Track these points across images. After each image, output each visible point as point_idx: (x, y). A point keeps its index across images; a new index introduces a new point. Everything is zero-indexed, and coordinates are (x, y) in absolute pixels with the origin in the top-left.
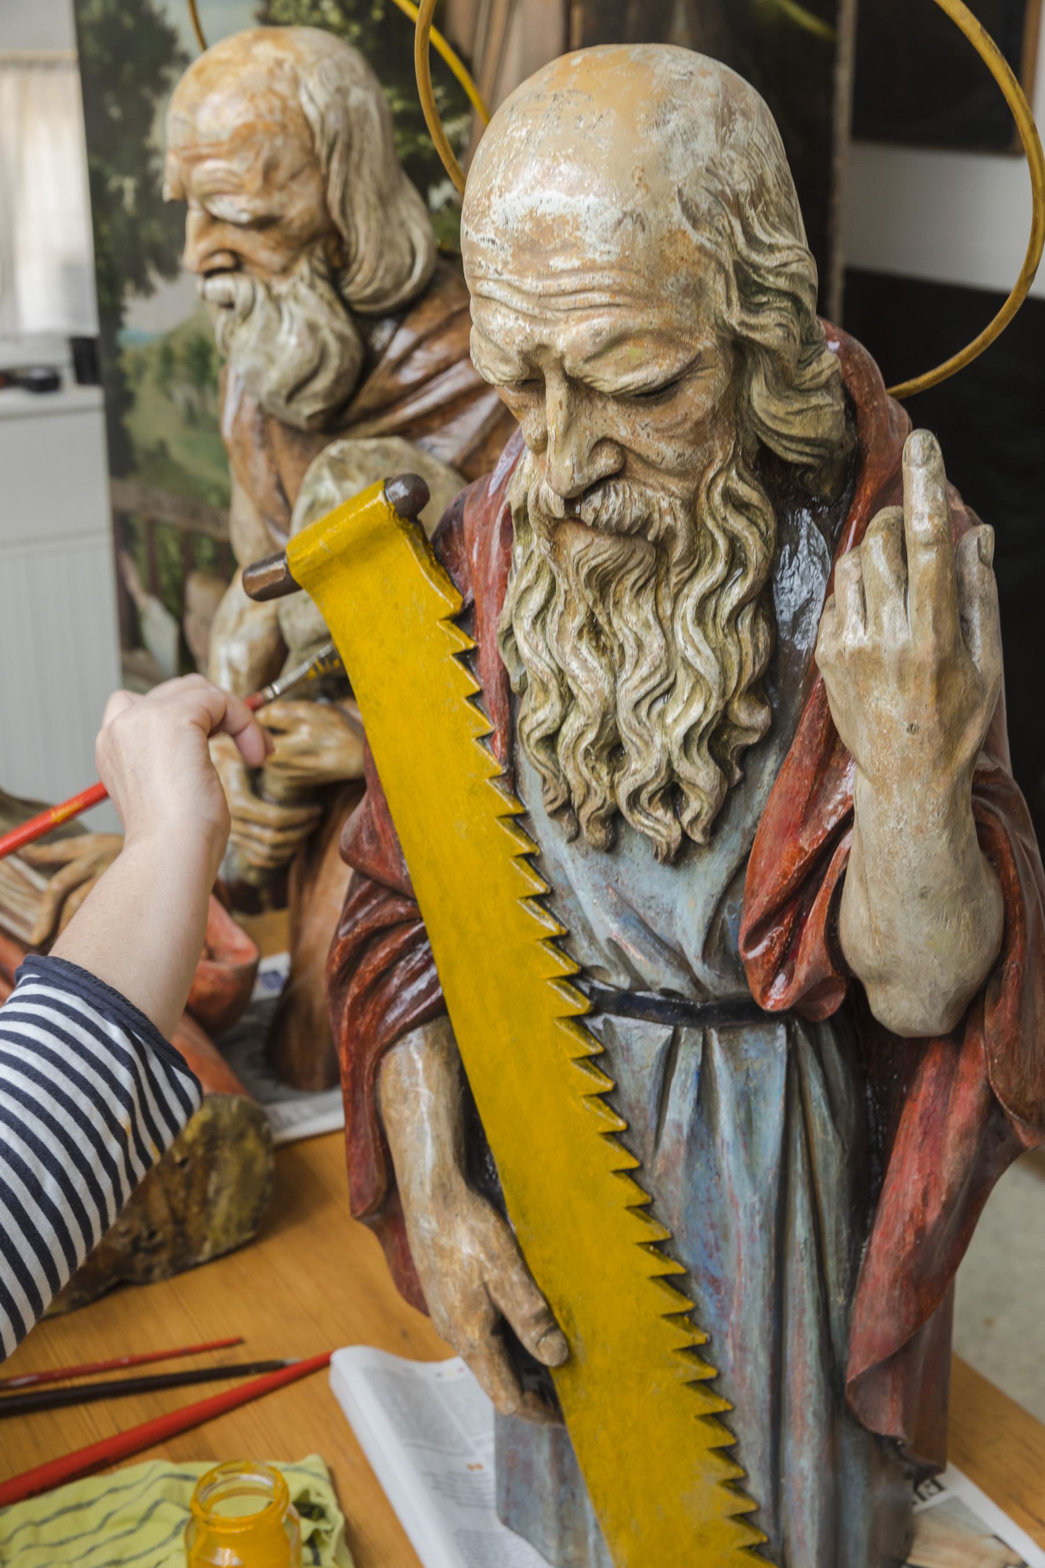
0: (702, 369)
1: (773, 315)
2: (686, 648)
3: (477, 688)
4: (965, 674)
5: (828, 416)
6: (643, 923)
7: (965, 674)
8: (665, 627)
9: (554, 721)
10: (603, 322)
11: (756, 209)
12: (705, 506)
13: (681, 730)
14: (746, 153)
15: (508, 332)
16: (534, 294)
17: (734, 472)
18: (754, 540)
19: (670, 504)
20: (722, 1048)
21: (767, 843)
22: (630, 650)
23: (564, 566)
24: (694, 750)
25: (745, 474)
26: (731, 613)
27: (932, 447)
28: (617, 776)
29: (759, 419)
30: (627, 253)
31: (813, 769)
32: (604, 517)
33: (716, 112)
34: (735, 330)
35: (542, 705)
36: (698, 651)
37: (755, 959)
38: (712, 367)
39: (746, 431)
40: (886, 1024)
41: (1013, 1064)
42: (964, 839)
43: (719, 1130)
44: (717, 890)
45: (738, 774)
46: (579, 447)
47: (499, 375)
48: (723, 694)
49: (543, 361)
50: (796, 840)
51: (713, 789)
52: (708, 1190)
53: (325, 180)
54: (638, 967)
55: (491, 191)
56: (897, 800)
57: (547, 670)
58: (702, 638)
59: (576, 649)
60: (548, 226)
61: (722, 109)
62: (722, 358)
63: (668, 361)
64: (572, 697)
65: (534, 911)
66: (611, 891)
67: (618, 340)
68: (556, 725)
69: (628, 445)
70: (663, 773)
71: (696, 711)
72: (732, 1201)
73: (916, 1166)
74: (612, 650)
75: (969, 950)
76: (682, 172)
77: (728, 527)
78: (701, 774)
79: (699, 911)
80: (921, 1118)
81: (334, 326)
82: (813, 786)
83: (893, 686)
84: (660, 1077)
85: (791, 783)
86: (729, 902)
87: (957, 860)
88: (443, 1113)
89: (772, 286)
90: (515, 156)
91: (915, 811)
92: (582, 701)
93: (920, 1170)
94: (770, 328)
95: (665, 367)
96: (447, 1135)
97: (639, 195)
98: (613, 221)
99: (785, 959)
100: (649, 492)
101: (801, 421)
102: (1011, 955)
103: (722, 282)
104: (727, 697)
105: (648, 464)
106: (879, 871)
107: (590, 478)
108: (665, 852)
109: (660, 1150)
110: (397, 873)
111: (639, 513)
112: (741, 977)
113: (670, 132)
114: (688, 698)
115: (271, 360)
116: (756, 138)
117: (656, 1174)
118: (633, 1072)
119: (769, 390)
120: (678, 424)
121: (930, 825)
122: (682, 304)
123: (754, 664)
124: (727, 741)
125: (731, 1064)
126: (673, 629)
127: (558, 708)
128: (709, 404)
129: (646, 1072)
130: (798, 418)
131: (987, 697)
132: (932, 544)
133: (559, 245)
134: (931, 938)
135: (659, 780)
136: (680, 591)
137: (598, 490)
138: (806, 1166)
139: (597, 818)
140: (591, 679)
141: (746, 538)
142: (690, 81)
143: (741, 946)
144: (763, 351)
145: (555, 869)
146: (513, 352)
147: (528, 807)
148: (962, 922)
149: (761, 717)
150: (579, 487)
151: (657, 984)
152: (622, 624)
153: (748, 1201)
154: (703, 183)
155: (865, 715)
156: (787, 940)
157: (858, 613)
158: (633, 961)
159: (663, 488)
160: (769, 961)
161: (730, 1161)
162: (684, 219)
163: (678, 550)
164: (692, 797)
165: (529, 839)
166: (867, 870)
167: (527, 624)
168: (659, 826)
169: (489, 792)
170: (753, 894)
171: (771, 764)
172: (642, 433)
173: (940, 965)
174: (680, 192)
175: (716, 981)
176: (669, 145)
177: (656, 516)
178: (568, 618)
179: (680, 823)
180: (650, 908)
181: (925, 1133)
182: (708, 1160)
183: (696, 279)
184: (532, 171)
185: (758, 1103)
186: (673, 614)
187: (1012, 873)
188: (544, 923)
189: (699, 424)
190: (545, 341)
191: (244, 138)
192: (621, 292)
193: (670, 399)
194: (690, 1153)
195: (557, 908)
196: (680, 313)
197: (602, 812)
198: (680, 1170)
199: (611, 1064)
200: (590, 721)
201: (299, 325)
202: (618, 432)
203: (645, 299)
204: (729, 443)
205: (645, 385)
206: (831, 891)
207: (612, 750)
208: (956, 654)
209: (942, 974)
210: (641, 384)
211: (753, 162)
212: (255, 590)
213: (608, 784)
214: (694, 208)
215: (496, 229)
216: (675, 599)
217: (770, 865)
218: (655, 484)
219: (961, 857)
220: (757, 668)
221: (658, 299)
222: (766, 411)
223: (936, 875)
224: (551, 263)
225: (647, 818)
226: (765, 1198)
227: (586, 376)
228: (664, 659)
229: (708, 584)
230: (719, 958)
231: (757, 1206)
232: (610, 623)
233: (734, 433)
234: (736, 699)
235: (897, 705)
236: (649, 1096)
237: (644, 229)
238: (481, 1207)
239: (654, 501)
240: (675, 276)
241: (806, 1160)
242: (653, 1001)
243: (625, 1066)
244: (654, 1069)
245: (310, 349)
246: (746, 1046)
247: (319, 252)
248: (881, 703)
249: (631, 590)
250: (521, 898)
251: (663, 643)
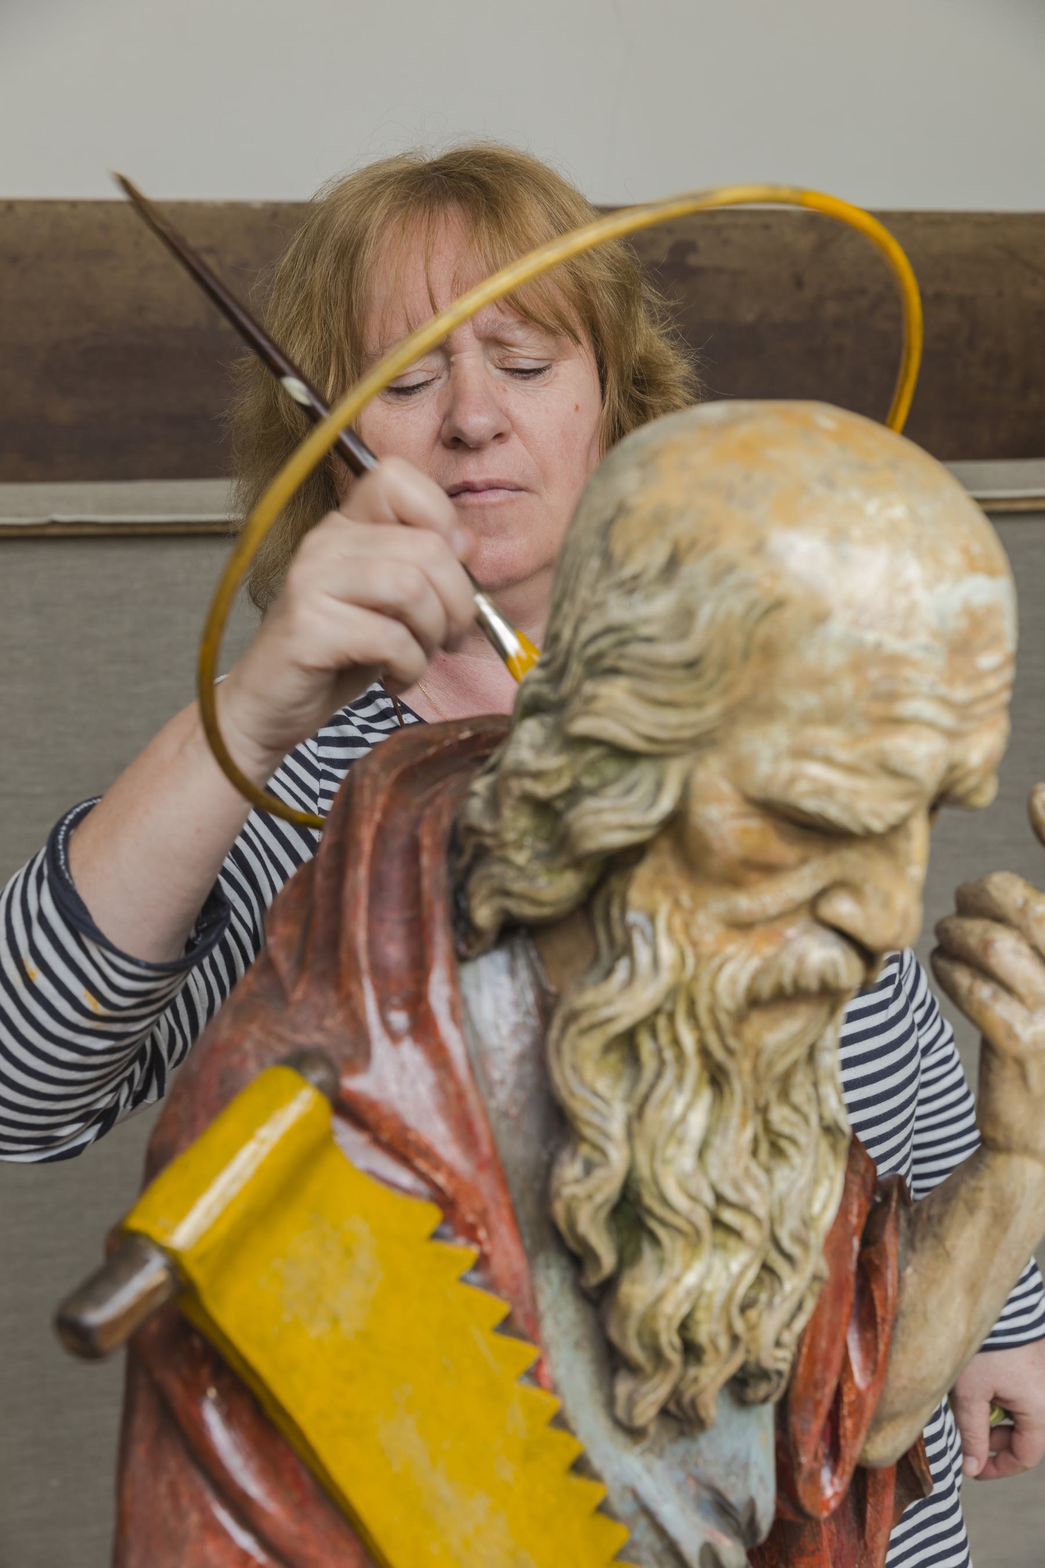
28: (752, 1314)
35: (687, 1267)
167: (687, 1161)
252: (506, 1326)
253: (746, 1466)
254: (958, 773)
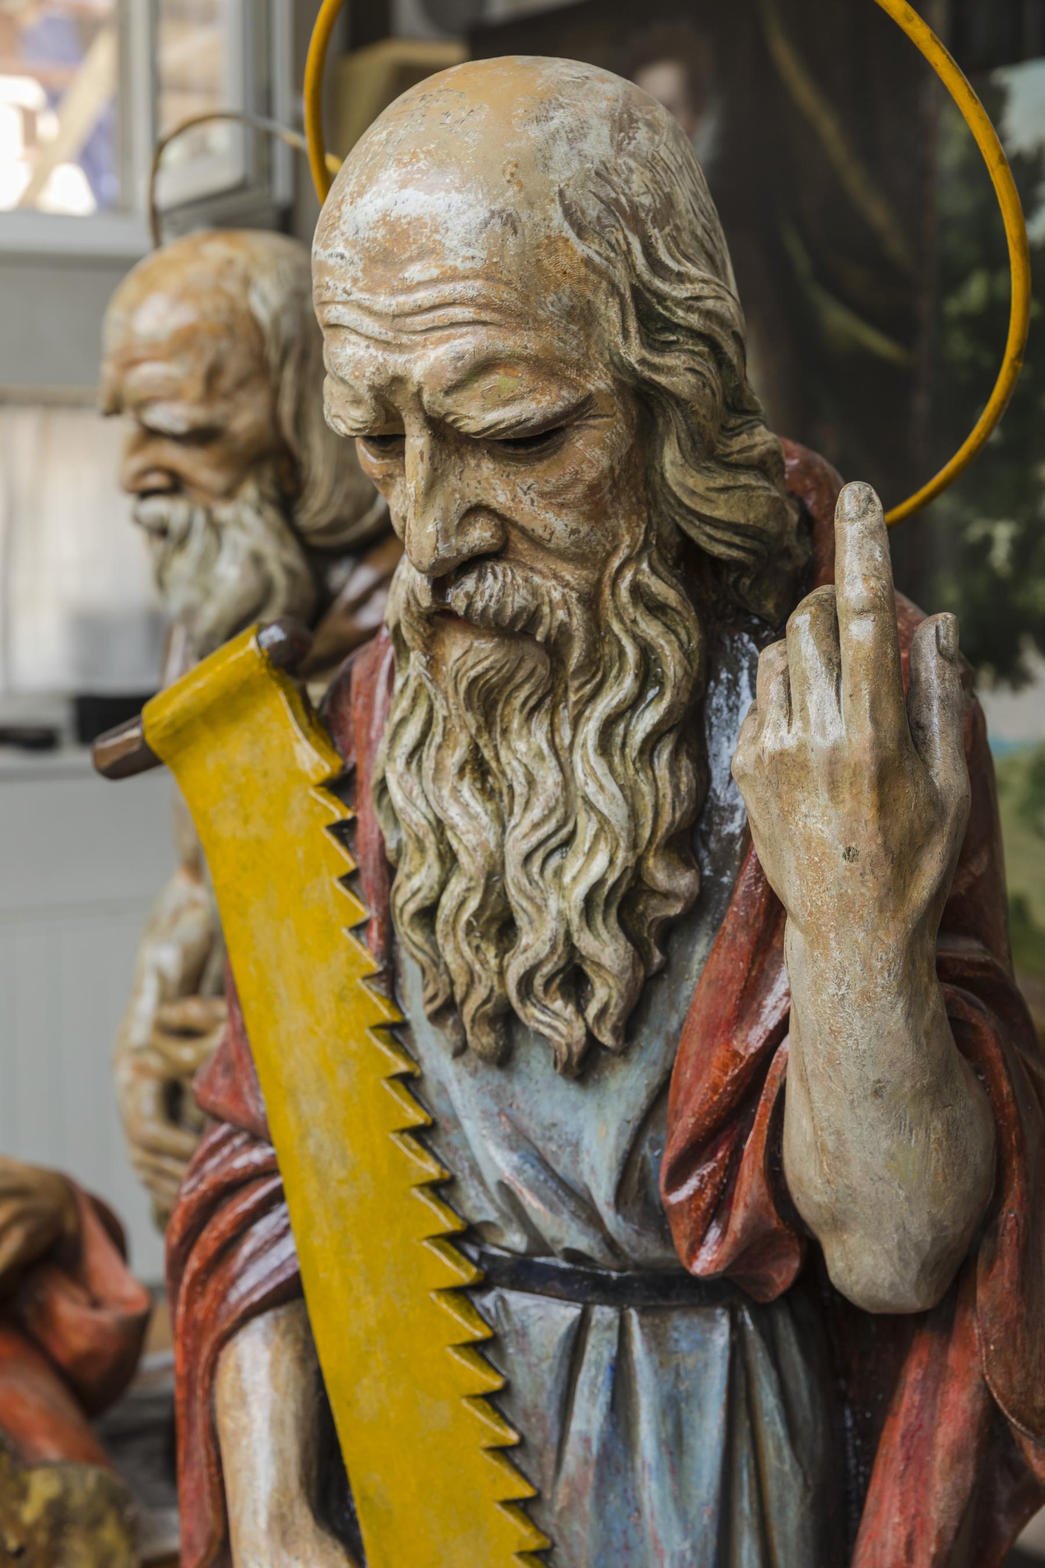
0: (594, 417)
1: (683, 358)
2: (587, 784)
3: (352, 865)
4: (917, 784)
5: (762, 499)
6: (543, 1163)
7: (917, 784)
8: (563, 760)
9: (432, 888)
10: (468, 343)
11: (661, 230)
12: (610, 604)
13: (580, 891)
14: (651, 164)
15: (358, 364)
16: (387, 314)
17: (645, 566)
18: (672, 651)
19: (564, 595)
20: (644, 1334)
21: (693, 1046)
22: (520, 789)
23: (443, 686)
24: (599, 919)
25: (661, 569)
26: (645, 741)
27: (870, 500)
28: (507, 956)
29: (674, 495)
30: (495, 260)
31: (748, 947)
32: (479, 605)
33: (612, 116)
34: (634, 369)
35: (418, 869)
36: (601, 787)
37: (680, 1204)
38: (607, 416)
39: (661, 514)
40: (846, 1293)
41: (1015, 1352)
42: (928, 1014)
43: (639, 1449)
44: (635, 1114)
45: (657, 957)
46: (446, 511)
47: (351, 423)
48: (634, 845)
49: (400, 400)
50: (728, 1042)
51: (623, 971)
52: (625, 1532)
53: (276, 393)
54: (535, 1219)
55: (342, 200)
56: (836, 954)
57: (424, 822)
58: (607, 771)
59: (455, 791)
60: (404, 231)
61: (621, 114)
62: (620, 406)
63: (548, 398)
64: (454, 858)
65: (410, 1149)
66: (504, 1119)
67: (484, 366)
68: (434, 894)
69: (508, 514)
70: (560, 949)
71: (599, 864)
72: (656, 1548)
73: (897, 1504)
74: (501, 794)
75: (945, 1180)
76: (564, 171)
77: (639, 632)
78: (606, 950)
79: (611, 1141)
80: (903, 1437)
81: (281, 559)
82: (750, 970)
83: (824, 797)
84: (564, 1373)
85: (722, 966)
86: (651, 1134)
87: (918, 1043)
88: (290, 1421)
89: (682, 322)
90: (372, 159)
91: (858, 969)
92: (463, 858)
93: (902, 1510)
94: (678, 372)
95: (544, 404)
96: (293, 1451)
97: (510, 193)
98: (478, 221)
99: (719, 1207)
100: (537, 579)
101: (727, 501)
102: (1008, 1201)
103: (616, 308)
104: (640, 851)
105: (537, 543)
106: (821, 1061)
107: (459, 551)
108: (565, 1058)
109: (563, 1476)
110: (253, 1110)
111: (523, 602)
112: (666, 1238)
113: (552, 129)
114: (590, 849)
115: (207, 593)
116: (664, 153)
117: (557, 1508)
118: (529, 1366)
119: (684, 457)
120: (567, 487)
121: (879, 990)
122: (567, 331)
123: (674, 809)
124: (643, 914)
125: (656, 1357)
126: (571, 762)
127: (436, 871)
128: (605, 463)
129: (545, 1366)
130: (723, 497)
131: (949, 820)
132: (868, 611)
133: (415, 252)
134: (893, 1157)
135: (555, 958)
136: (581, 714)
137: (472, 572)
138: (755, 1506)
139: (485, 1015)
140: (474, 827)
141: (662, 647)
142: (584, 84)
143: (662, 1187)
144: (673, 403)
145: (438, 1094)
146: (363, 389)
147: (408, 1016)
148: (933, 1136)
149: (685, 881)
150: (445, 560)
151: (560, 1242)
152: (510, 756)
153: (677, 1549)
154: (592, 188)
155: (791, 840)
156: (721, 1182)
157: (782, 707)
158: (529, 1211)
159: (556, 576)
160: (698, 1208)
161: (652, 1491)
162: (566, 225)
163: (576, 655)
164: (597, 982)
165: (407, 1056)
166: (807, 1060)
167: (400, 764)
169: (360, 996)
170: (677, 1115)
171: (701, 949)
172: (524, 498)
173: (907, 1198)
174: (561, 193)
175: (634, 1238)
176: (551, 142)
177: (546, 609)
178: (446, 752)
179: (585, 1020)
180: (551, 1139)
181: (908, 1458)
182: (625, 1491)
183: (584, 301)
184: (390, 175)
185: (691, 1412)
186: (572, 743)
187: (1006, 1089)
188: (420, 1163)
189: (594, 488)
190: (400, 372)
191: (184, 341)
192: (487, 306)
193: (555, 452)
194: (601, 1480)
195: (439, 1146)
196: (564, 342)
197: (489, 1006)
198: (587, 1503)
199: (502, 1354)
200: (473, 884)
201: (242, 555)
202: (495, 497)
203: (518, 317)
204: (638, 526)
205: (519, 423)
206: (770, 1105)
207: (501, 926)
208: (902, 756)
209: (912, 1213)
210: (513, 421)
211: (658, 177)
212: (105, 763)
213: (496, 969)
214: (579, 214)
215: (346, 241)
216: (576, 723)
217: (698, 1076)
218: (545, 570)
219: (923, 1040)
220: (678, 815)
221: (535, 320)
222: (682, 485)
223: (892, 1064)
224: (406, 275)
225: (543, 1012)
226: (699, 1546)
227: (448, 414)
228: (561, 799)
229: (614, 703)
230: (638, 1209)
231: (689, 1555)
232: (498, 759)
233: (645, 515)
234: (652, 853)
235: (829, 822)
236: (549, 1398)
237: (515, 232)
238: (331, 1550)
239: (544, 590)
240: (555, 293)
241: (755, 1496)
242: (556, 1269)
243: (520, 1358)
244: (557, 1361)
245: (252, 582)
246: (676, 1335)
247: (268, 473)
248: (811, 821)
249: (521, 711)
250: (395, 1131)
251: (559, 778)
252: (350, 879)
253: (576, 1146)
254: (412, 389)
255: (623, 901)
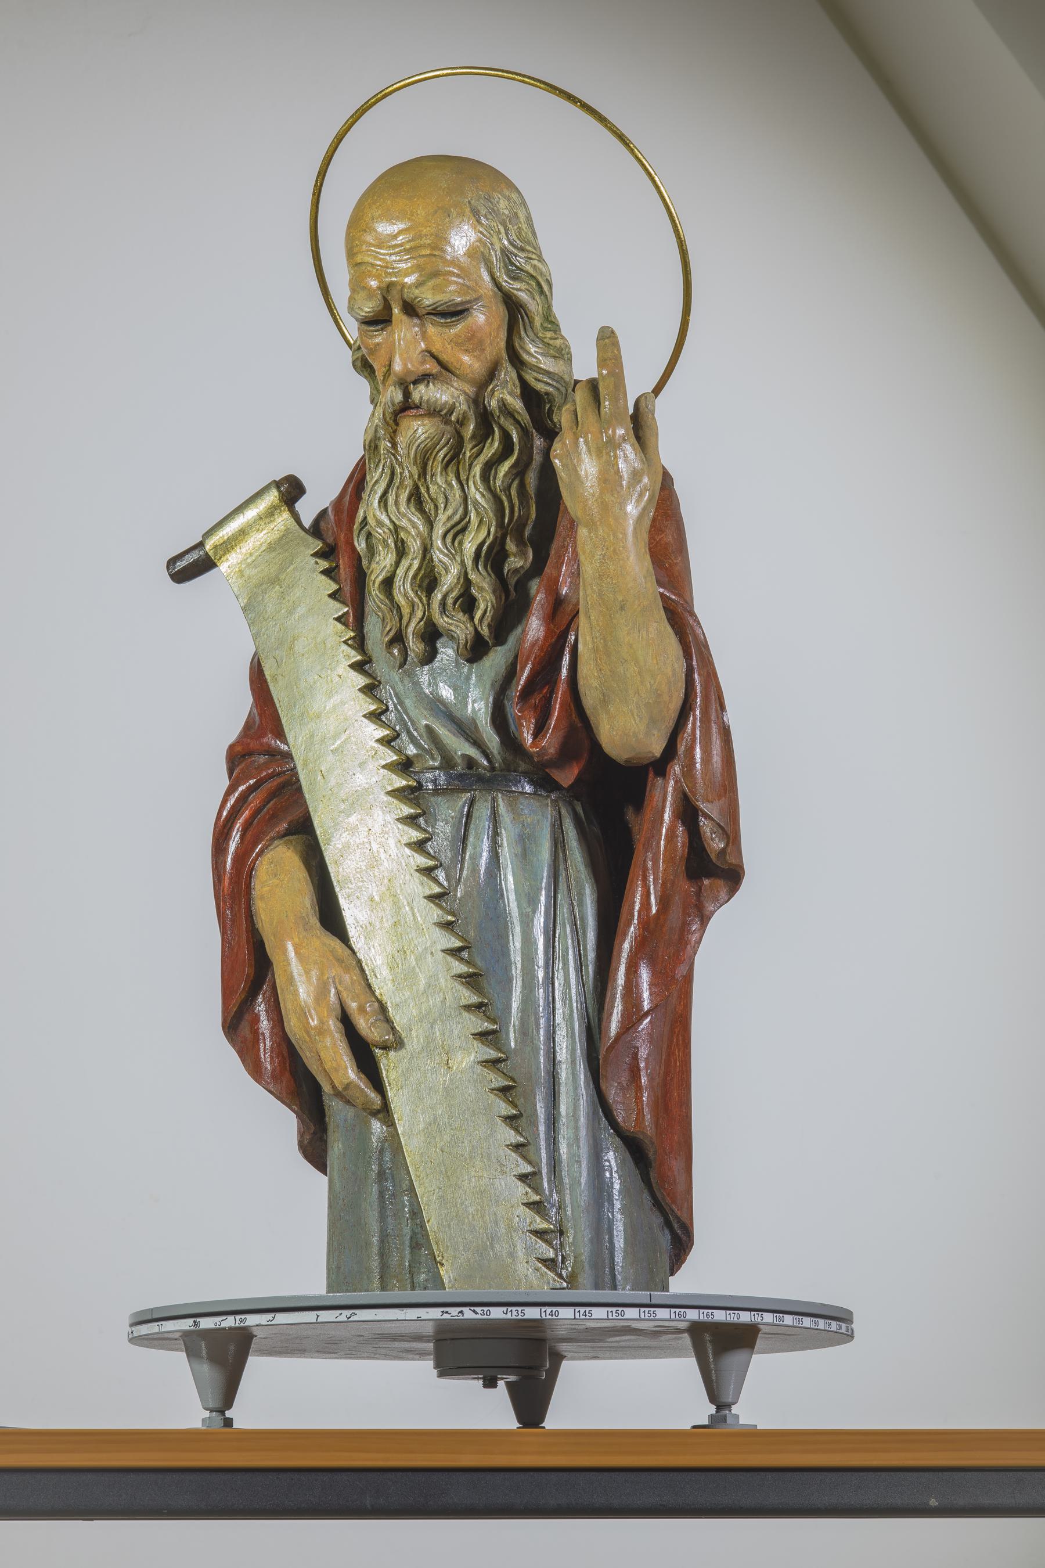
70: (462, 581)
168: (459, 626)
207: (428, 581)
227: (417, 297)
255: (493, 557)
